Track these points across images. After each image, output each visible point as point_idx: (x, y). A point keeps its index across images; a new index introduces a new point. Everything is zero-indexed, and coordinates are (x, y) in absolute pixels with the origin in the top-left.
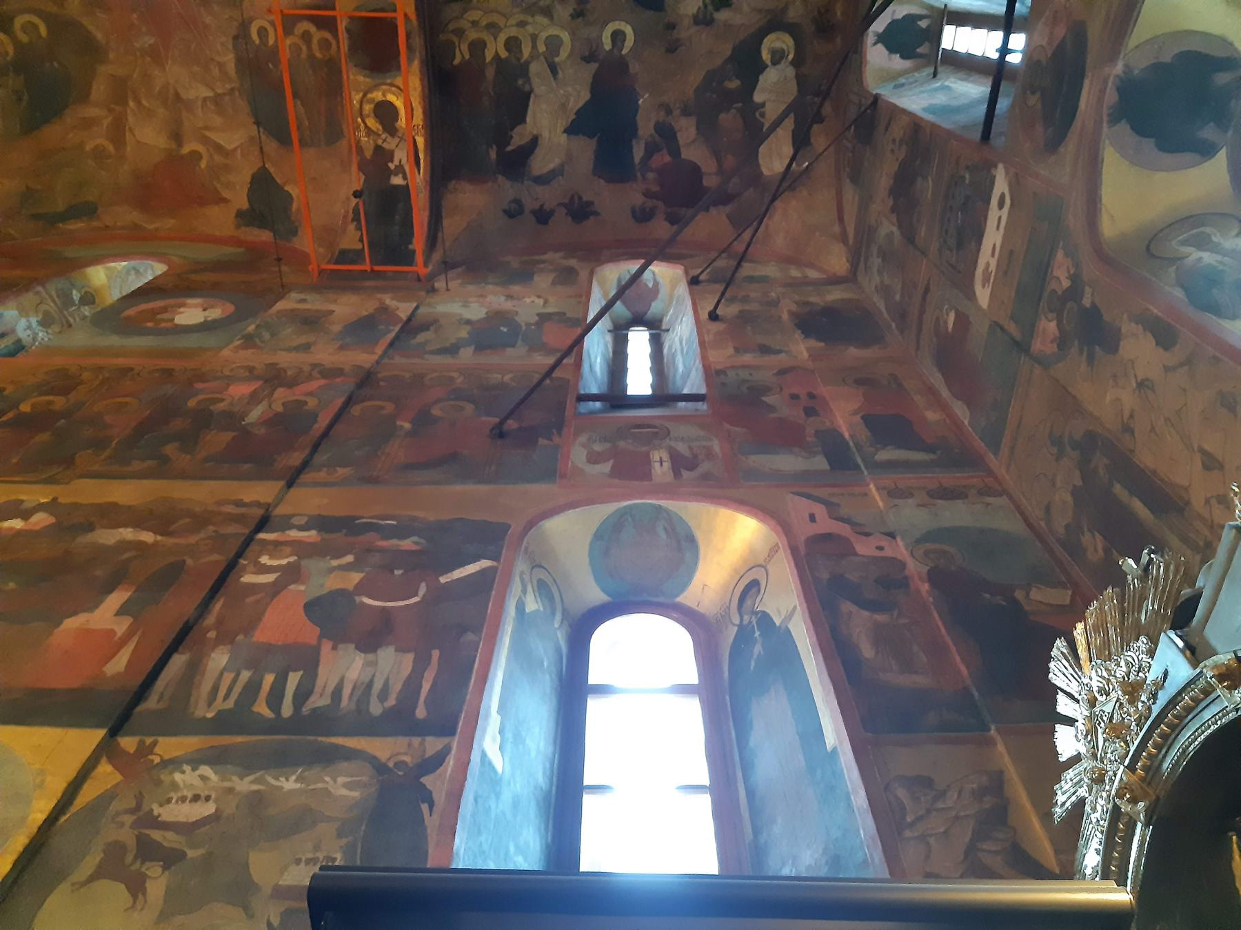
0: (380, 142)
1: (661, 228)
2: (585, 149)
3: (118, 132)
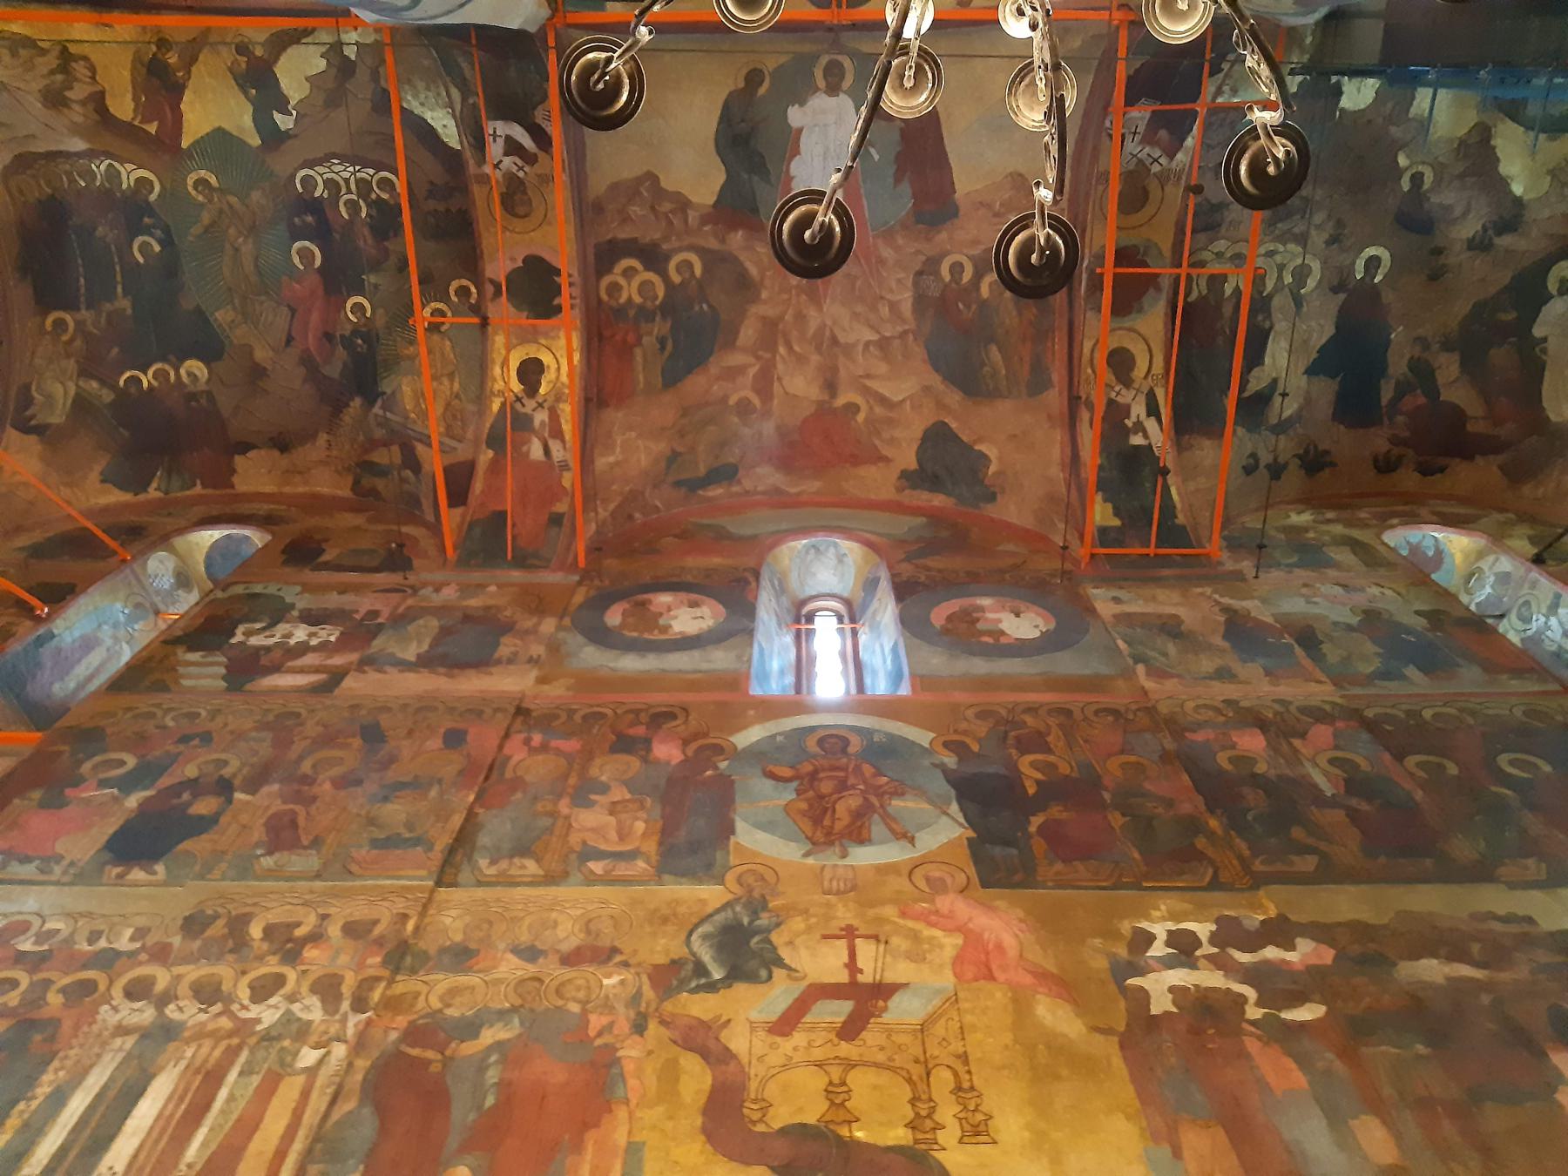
0: (1113, 395)
1: (1408, 479)
2: (1326, 390)
3: (764, 384)
